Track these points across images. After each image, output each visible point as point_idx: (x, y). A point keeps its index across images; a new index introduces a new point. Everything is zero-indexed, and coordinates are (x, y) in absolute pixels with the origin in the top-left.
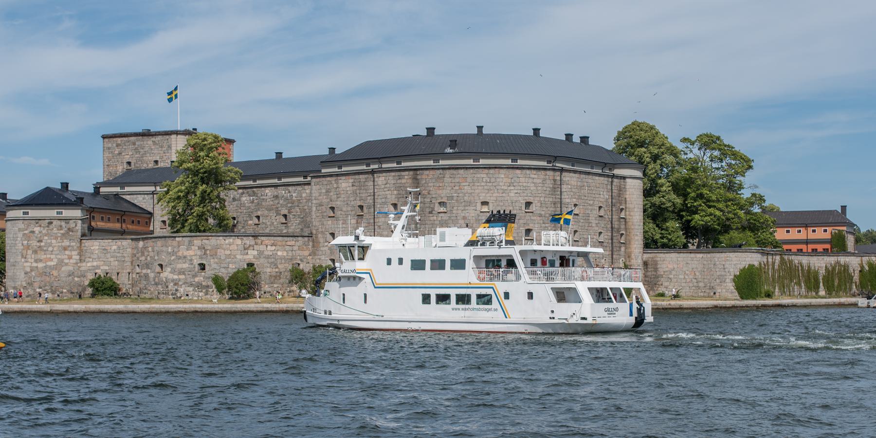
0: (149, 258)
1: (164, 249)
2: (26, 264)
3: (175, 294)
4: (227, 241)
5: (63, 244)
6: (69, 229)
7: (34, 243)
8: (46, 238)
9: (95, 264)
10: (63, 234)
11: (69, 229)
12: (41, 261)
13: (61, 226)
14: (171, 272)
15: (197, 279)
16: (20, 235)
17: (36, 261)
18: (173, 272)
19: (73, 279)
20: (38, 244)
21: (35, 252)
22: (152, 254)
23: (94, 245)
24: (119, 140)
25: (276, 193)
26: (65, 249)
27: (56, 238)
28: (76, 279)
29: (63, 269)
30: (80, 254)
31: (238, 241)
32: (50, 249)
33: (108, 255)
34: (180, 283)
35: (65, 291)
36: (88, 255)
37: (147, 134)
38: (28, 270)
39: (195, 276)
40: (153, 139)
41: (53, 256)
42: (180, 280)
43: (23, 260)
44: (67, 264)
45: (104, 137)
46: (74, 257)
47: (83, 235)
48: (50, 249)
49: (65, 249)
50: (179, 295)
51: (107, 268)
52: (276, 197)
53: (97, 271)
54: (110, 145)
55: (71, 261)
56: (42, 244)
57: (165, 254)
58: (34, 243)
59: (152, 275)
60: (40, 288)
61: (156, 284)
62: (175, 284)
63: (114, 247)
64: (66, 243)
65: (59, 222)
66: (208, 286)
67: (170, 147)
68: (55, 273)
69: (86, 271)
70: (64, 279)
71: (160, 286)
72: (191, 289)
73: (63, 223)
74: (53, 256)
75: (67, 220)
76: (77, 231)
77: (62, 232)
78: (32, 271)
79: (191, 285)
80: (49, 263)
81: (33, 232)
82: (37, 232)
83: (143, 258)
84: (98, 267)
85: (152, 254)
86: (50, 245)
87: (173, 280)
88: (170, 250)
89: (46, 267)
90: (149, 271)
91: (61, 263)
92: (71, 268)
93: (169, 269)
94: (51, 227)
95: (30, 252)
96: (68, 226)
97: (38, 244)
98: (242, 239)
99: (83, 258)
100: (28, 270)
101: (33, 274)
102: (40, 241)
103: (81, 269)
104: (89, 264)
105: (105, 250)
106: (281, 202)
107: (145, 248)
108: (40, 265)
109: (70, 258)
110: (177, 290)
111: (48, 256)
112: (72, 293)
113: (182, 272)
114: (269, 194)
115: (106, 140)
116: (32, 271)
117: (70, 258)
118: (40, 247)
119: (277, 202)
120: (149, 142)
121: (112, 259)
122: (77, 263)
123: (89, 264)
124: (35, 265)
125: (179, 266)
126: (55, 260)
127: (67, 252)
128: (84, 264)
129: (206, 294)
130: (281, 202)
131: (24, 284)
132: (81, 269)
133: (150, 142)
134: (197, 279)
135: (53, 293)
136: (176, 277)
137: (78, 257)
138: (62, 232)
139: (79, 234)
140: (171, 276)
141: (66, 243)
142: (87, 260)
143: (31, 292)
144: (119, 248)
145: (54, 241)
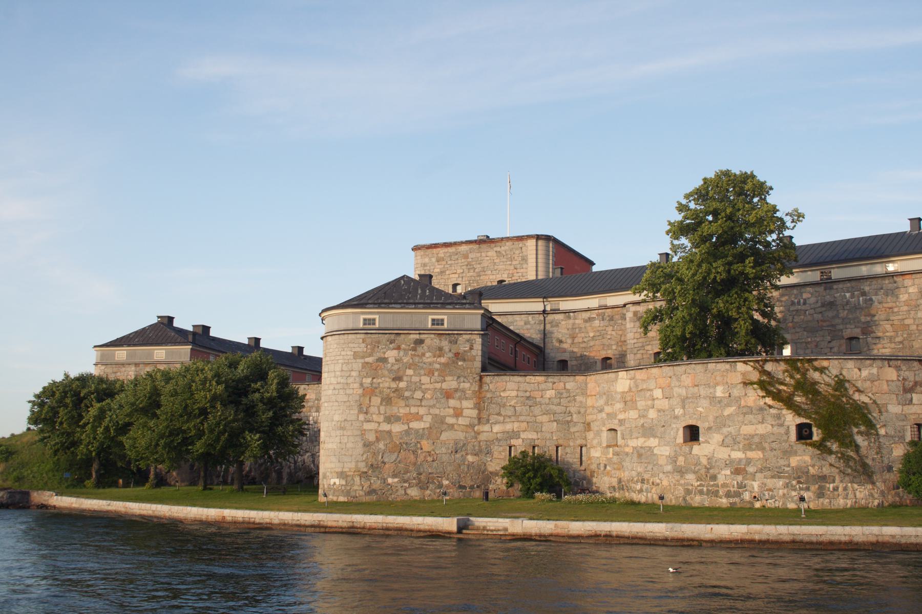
0: (652, 414)
1: (703, 391)
2: (367, 426)
3: (738, 494)
4: (865, 373)
5: (445, 386)
6: (457, 355)
7: (386, 383)
8: (410, 372)
9: (509, 427)
10: (445, 365)
11: (457, 355)
12: (398, 419)
13: (441, 349)
14: (723, 444)
15: (794, 461)
16: (358, 365)
17: (389, 420)
18: (731, 442)
19: (464, 458)
20: (394, 385)
21: (387, 401)
22: (664, 404)
23: (509, 387)
24: (442, 252)
25: (828, 298)
26: (448, 395)
27: (430, 373)
28: (470, 458)
29: (444, 436)
30: (478, 407)
31: (891, 374)
32: (418, 395)
33: (537, 410)
34: (751, 469)
35: (446, 482)
36: (494, 408)
37: (485, 241)
38: (371, 437)
39: (788, 453)
40: (498, 249)
41: (422, 411)
42: (749, 461)
43: (362, 417)
44: (451, 427)
45: (416, 248)
46: (466, 412)
47: (484, 369)
48: (418, 395)
49: (448, 395)
50: (747, 496)
51: (532, 435)
52: (831, 305)
53: (513, 442)
54: (427, 260)
55: (461, 421)
56: (402, 385)
57: (705, 403)
58: (386, 383)
59: (663, 451)
60: (394, 476)
61: (681, 472)
62: (737, 472)
63: (550, 393)
64: (451, 383)
65: (437, 341)
66: (823, 478)
67: (525, 259)
68: (426, 445)
69: (489, 443)
70: (445, 458)
71: (691, 477)
72: (781, 483)
73: (445, 344)
74: (422, 411)
75: (452, 335)
76: (473, 359)
77: (443, 360)
78: (378, 440)
79: (778, 475)
80: (415, 425)
81: (384, 360)
82: (392, 360)
83: (633, 414)
84: (515, 434)
85: (664, 404)
86: (419, 386)
87: (729, 463)
88: (719, 392)
89: (408, 432)
90: (653, 442)
91: (439, 423)
92: (460, 435)
93: (717, 438)
94: (420, 350)
95: (376, 400)
96: (455, 349)
97: (394, 385)
98: (898, 368)
99: (484, 415)
100: (371, 437)
101: (381, 445)
102: (398, 379)
103: (483, 437)
104: (496, 428)
105: (529, 399)
106: (843, 314)
107: (638, 390)
108: (397, 428)
109: (458, 413)
110: (741, 486)
111: (414, 410)
112: (462, 487)
113: (750, 444)
114: (813, 300)
115: (419, 252)
116: (378, 440)
117: (458, 413)
118: (397, 390)
119: (830, 314)
120: (490, 253)
121: (545, 418)
122: (472, 426)
123: (496, 428)
124: (385, 427)
125: (747, 430)
126: (428, 419)
127: (452, 402)
128: (486, 428)
129: (820, 494)
130: (843, 314)
131: (363, 467)
132: (483, 437)
133: (492, 253)
134: (794, 461)
135: (423, 486)
136: (738, 455)
137: (474, 413)
138: (443, 360)
139: (478, 364)
140: (723, 454)
141: (451, 383)
142: (493, 418)
143: (377, 484)
144: (559, 395)
145: (425, 379)
